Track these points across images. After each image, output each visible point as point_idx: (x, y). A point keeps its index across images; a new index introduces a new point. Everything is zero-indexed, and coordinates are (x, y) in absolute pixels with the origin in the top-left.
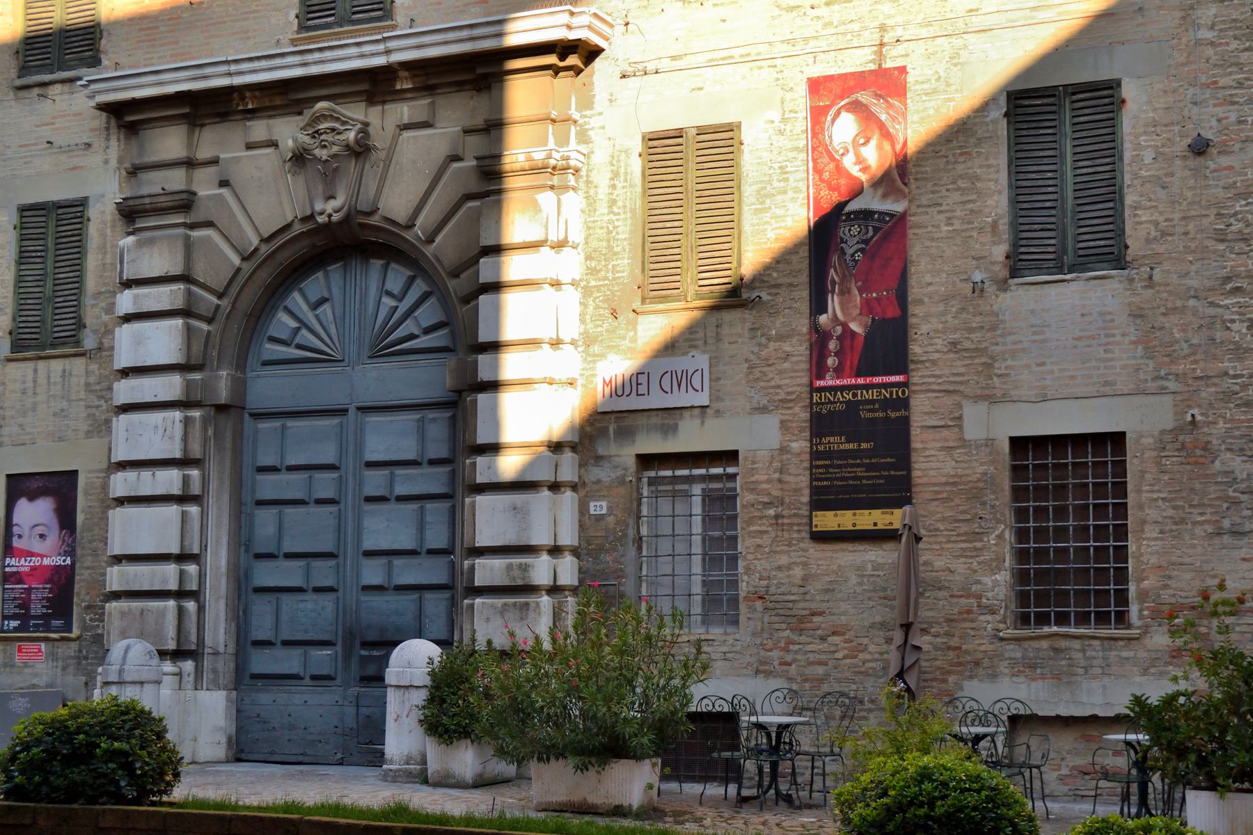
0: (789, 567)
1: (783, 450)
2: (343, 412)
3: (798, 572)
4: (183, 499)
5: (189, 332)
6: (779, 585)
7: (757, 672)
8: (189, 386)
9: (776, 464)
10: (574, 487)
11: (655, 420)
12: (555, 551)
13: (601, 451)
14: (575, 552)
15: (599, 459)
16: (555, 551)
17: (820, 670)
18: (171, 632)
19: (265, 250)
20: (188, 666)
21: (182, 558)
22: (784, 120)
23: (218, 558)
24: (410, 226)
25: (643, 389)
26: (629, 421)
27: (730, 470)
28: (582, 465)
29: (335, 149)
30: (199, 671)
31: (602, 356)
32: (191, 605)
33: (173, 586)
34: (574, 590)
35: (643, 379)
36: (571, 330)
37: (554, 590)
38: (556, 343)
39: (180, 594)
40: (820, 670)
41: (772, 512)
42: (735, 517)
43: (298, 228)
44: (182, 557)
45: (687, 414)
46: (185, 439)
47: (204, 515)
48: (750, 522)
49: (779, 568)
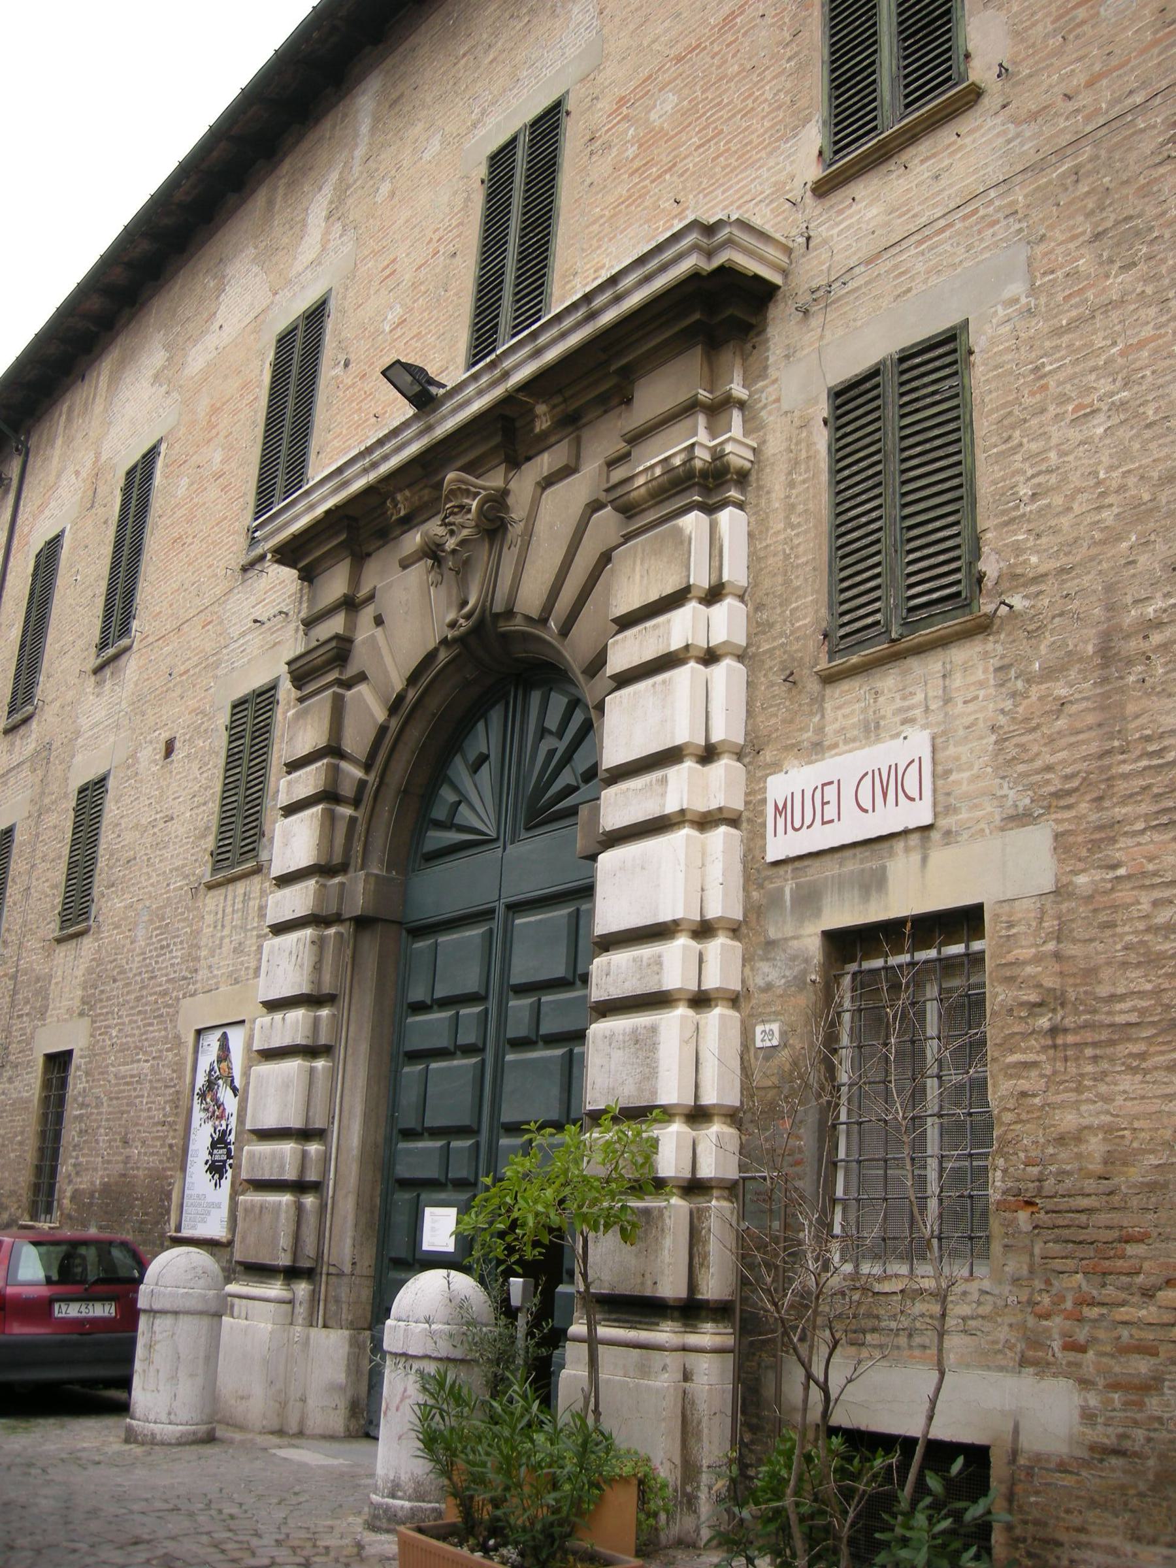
0: (1078, 1137)
1: (1061, 892)
2: (486, 915)
3: (1095, 1146)
4: (310, 1051)
5: (330, 819)
6: (1062, 1174)
7: (1024, 1362)
8: (321, 894)
9: (1050, 924)
10: (734, 1001)
11: (852, 865)
12: (698, 1115)
13: (773, 933)
14: (733, 1116)
15: (770, 944)
16: (698, 1115)
17: (1142, 1366)
18: (285, 1241)
19: (412, 695)
20: (302, 1288)
21: (305, 1135)
22: (1033, 291)
23: (351, 1135)
24: (543, 621)
25: (830, 812)
26: (816, 872)
27: (977, 946)
28: (747, 960)
29: (465, 532)
30: (314, 1298)
31: (776, 767)
32: (309, 1200)
33: (290, 1175)
34: (731, 1189)
35: (831, 793)
36: (726, 727)
37: (694, 1187)
38: (708, 754)
39: (300, 1187)
40: (1142, 1366)
41: (1044, 1022)
42: (983, 1042)
43: (443, 656)
44: (305, 1135)
45: (899, 845)
46: (317, 967)
47: (333, 1071)
48: (1009, 1045)
49: (1061, 1140)
